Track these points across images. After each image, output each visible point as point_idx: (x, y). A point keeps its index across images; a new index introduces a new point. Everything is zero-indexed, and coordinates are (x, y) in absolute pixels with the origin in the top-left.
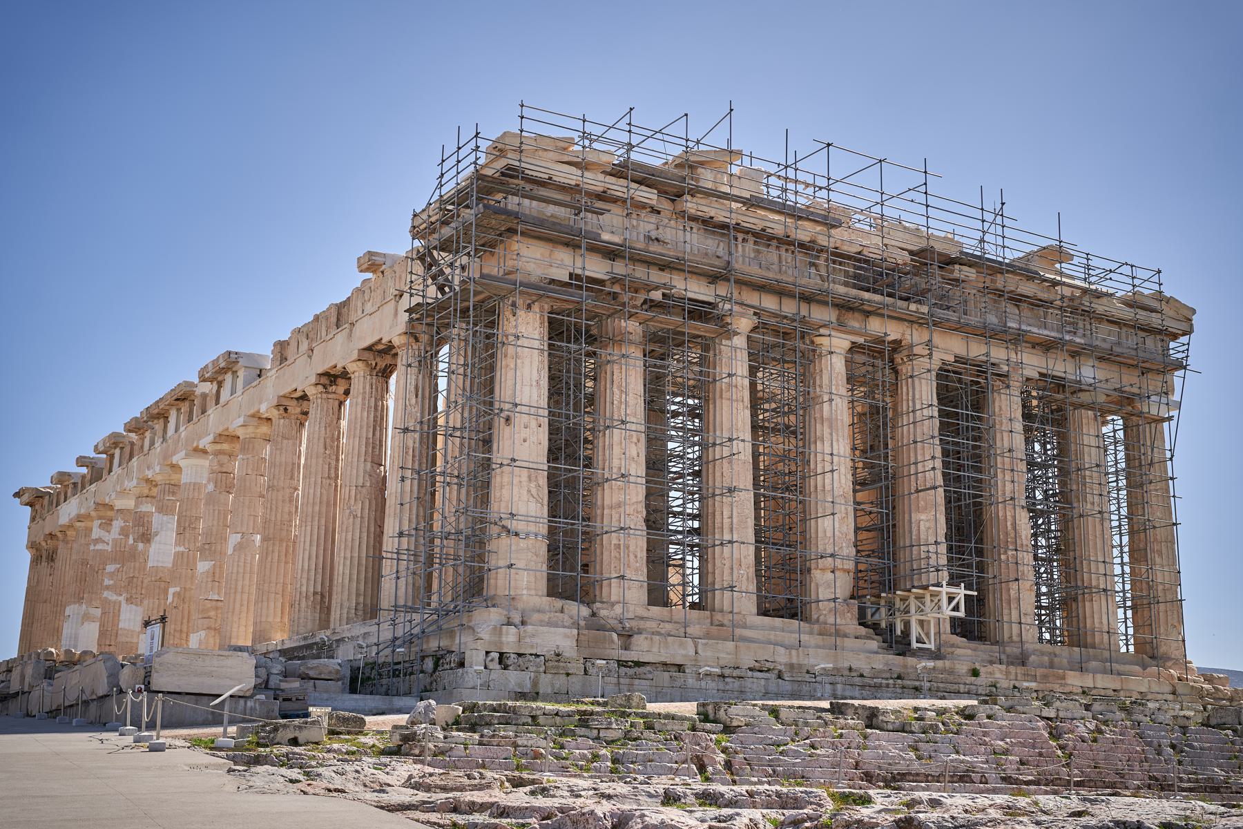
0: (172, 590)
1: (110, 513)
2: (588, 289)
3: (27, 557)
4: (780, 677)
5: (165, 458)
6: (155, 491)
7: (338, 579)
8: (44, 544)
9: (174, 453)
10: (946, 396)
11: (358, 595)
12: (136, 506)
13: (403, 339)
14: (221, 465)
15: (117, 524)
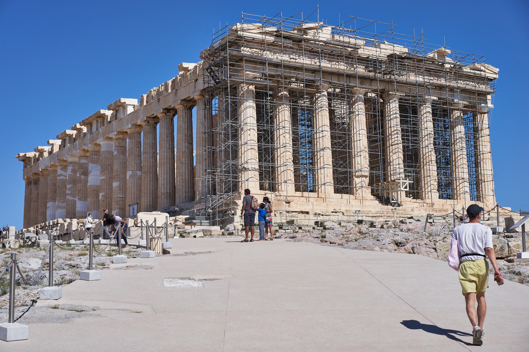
0: (101, 194)
1: (65, 164)
2: (270, 80)
3: (24, 183)
4: (343, 214)
5: (93, 141)
6: (88, 154)
7: (177, 187)
8: (32, 177)
9: (97, 139)
10: (402, 109)
11: (186, 193)
12: (79, 160)
13: (199, 97)
14: (120, 144)
15: (70, 168)
